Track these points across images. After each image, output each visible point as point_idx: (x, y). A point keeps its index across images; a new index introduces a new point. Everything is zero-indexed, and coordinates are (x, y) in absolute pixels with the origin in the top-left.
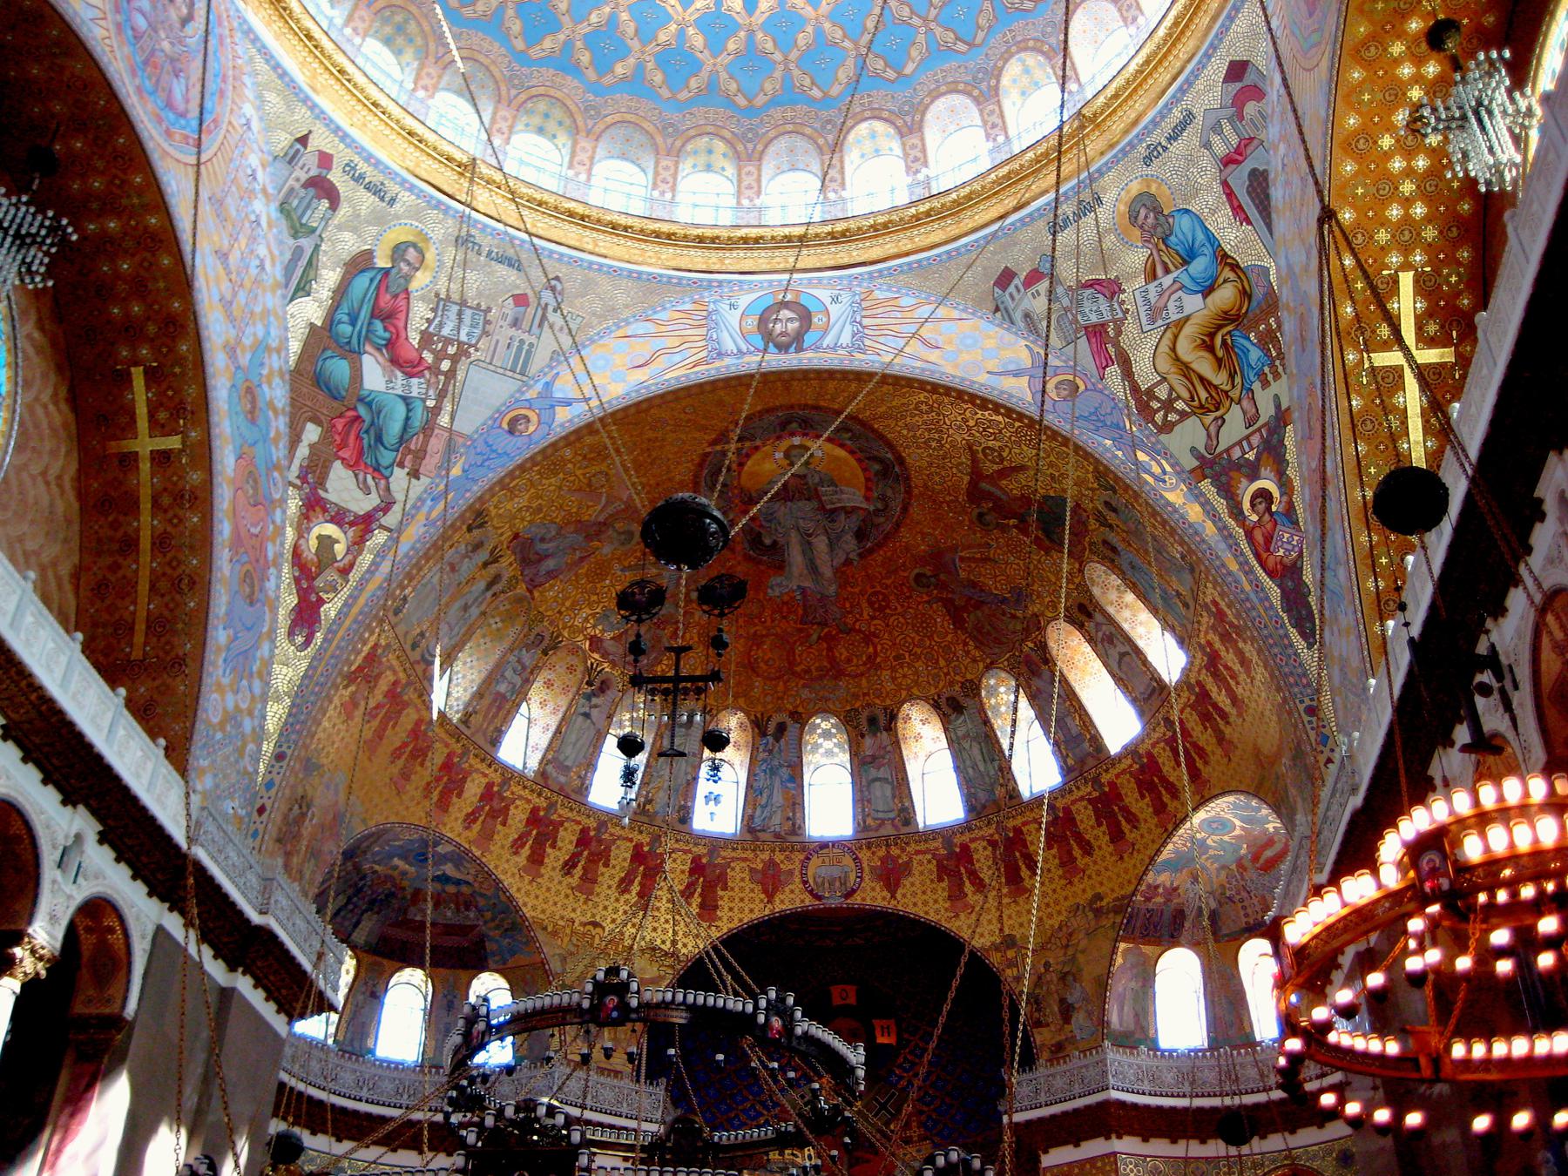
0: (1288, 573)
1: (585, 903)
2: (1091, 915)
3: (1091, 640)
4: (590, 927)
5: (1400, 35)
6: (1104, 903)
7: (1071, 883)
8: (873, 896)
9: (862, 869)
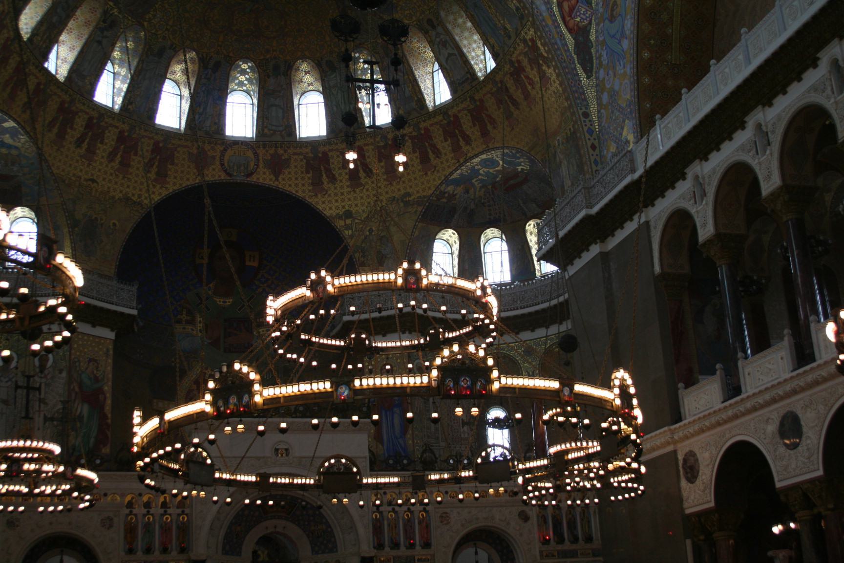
0: (581, 33)
1: (88, 166)
2: (402, 205)
3: (432, 44)
4: (90, 183)
6: (411, 199)
7: (391, 184)
8: (264, 177)
9: (258, 160)
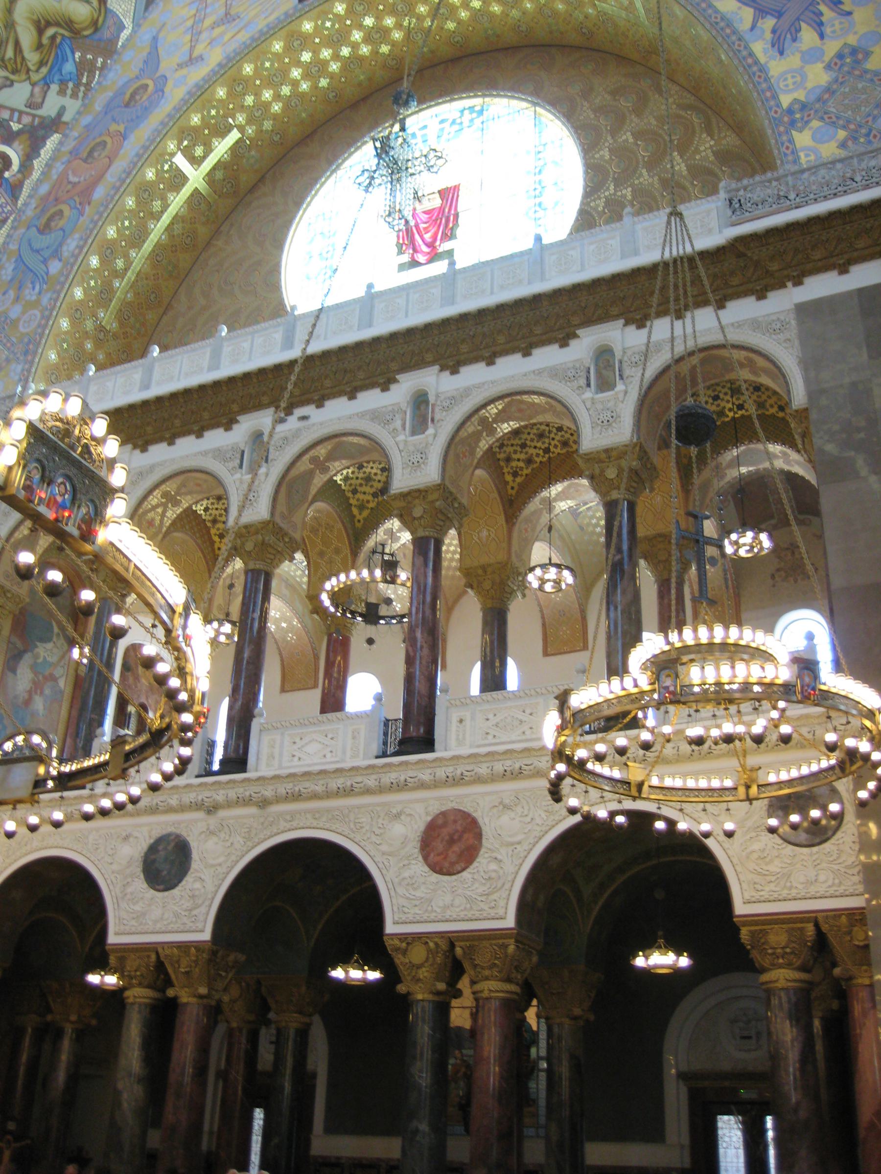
5: (379, 18)
